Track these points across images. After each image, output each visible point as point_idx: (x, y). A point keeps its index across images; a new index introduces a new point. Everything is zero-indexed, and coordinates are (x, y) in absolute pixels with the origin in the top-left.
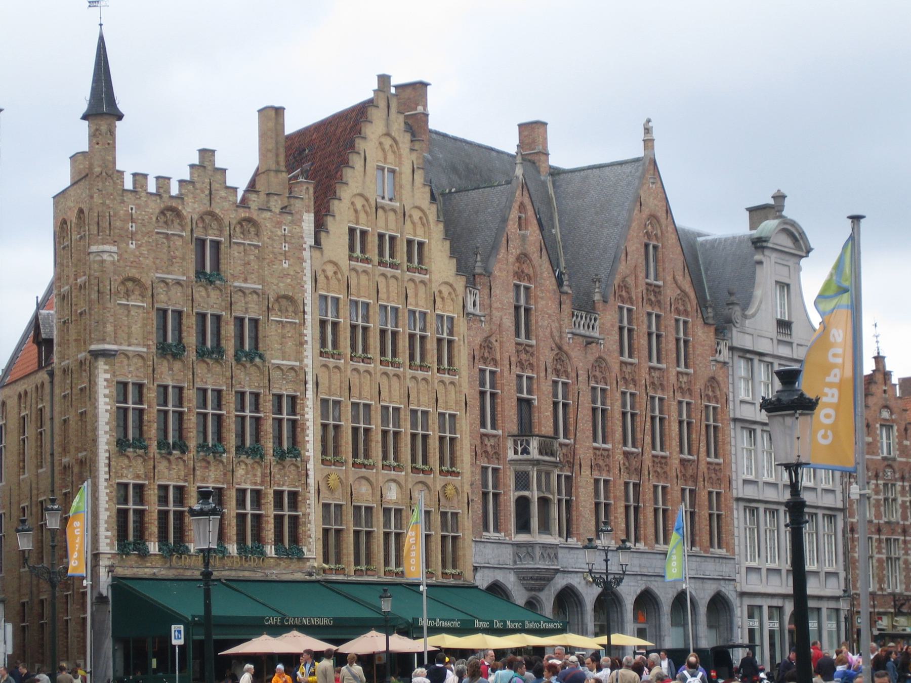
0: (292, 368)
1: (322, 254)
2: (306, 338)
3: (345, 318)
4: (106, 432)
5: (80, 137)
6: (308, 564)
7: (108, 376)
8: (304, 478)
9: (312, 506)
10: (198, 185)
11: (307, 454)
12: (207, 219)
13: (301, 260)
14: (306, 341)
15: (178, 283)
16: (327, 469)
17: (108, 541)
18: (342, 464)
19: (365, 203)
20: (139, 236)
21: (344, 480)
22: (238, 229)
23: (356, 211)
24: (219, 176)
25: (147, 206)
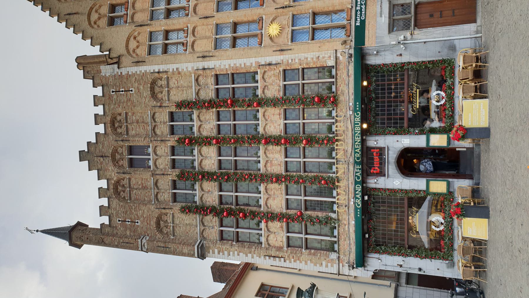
0: (197, 80)
1: (123, 55)
2: (175, 70)
3: (161, 26)
4: (253, 257)
5: (90, 250)
6: (341, 58)
7: (216, 251)
8: (272, 67)
9: (293, 56)
10: (99, 166)
11: (254, 65)
12: (118, 157)
13: (128, 76)
14: (177, 69)
15: (156, 184)
16: (266, 41)
17: (329, 264)
18: (261, 19)
19: (94, 10)
20: (133, 218)
21: (274, 16)
22: (119, 130)
23: (99, 18)
24: (92, 149)
25: (115, 209)
